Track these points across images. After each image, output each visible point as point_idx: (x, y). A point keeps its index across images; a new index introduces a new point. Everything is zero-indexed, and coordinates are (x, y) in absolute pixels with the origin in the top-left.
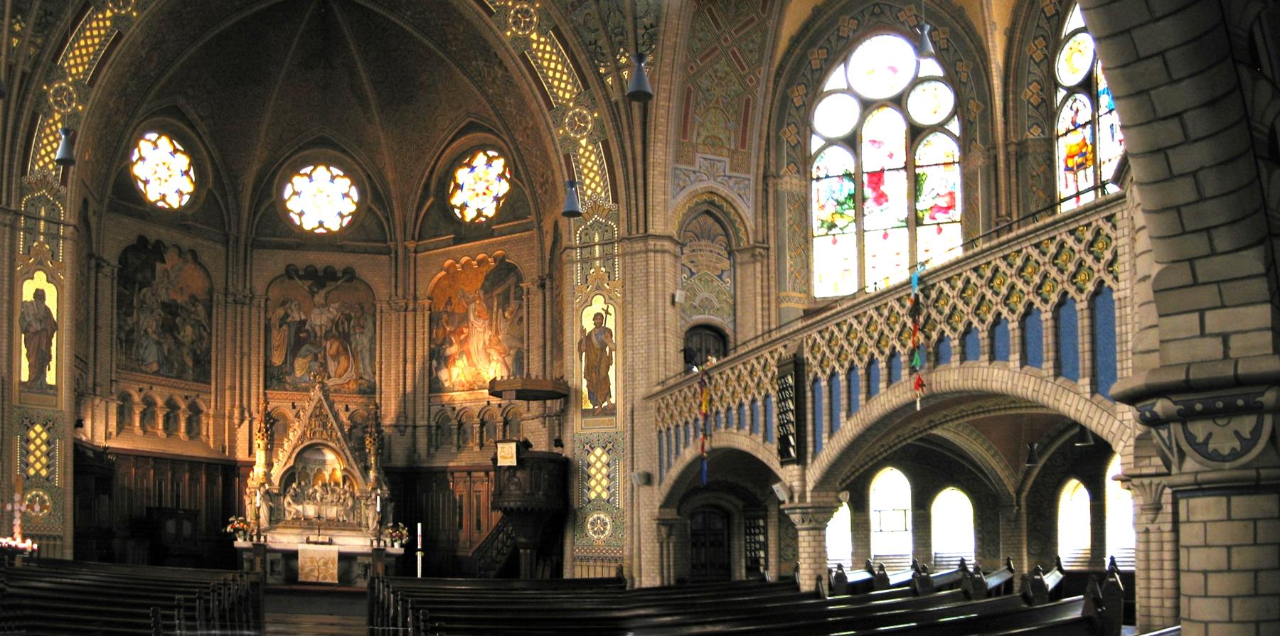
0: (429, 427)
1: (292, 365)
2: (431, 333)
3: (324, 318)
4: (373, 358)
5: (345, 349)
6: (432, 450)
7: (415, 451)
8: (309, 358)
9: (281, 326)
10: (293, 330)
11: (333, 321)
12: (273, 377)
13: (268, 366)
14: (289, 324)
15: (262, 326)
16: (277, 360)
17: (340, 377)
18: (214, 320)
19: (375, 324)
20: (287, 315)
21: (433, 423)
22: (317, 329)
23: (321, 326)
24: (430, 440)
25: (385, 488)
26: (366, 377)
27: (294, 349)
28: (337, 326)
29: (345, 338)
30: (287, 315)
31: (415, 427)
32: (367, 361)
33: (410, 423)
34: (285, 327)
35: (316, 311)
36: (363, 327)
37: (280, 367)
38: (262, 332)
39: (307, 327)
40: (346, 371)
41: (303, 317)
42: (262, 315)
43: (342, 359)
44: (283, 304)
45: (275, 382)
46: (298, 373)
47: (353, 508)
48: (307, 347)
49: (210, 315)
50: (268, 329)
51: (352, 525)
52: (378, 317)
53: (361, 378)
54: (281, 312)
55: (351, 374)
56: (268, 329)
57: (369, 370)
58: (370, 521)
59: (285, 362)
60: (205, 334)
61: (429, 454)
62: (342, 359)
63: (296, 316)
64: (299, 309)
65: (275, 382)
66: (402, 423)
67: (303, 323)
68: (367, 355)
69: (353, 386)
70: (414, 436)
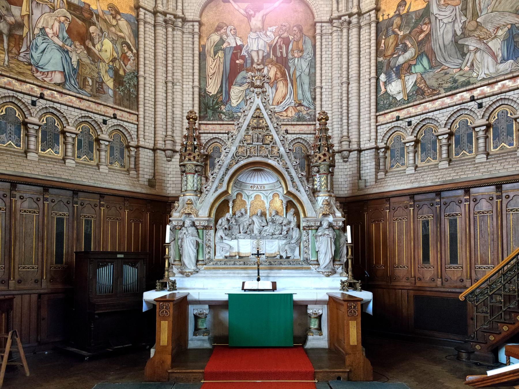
0: (377, 148)
1: (228, 94)
2: (378, 44)
3: (261, 43)
4: (312, 82)
5: (283, 75)
6: (381, 175)
7: (360, 178)
8: (246, 86)
9: (215, 53)
10: (229, 57)
11: (270, 46)
12: (207, 107)
13: (203, 94)
14: (224, 50)
15: (197, 52)
16: (212, 89)
17: (278, 104)
18: (141, 40)
19: (314, 46)
20: (222, 41)
21: (381, 145)
22: (254, 55)
23: (258, 52)
24: (378, 165)
25: (339, 214)
26: (305, 103)
27: (230, 77)
28: (275, 53)
29: (283, 63)
30: (222, 41)
31: (360, 151)
32: (306, 87)
33: (355, 146)
34: (220, 54)
35: (253, 35)
36: (302, 51)
37: (215, 96)
38: (197, 58)
39: (244, 53)
40: (284, 98)
41: (239, 43)
42: (196, 39)
43: (281, 85)
44: (218, 29)
45: (210, 112)
46: (234, 102)
47: (299, 241)
48: (243, 74)
49: (136, 35)
50: (202, 57)
51: (297, 262)
52: (318, 37)
53: (300, 105)
54: (215, 38)
55: (290, 100)
56: (202, 57)
57: (308, 95)
58: (321, 257)
59: (220, 91)
60: (129, 54)
61: (376, 178)
62: (281, 85)
63: (232, 42)
64: (235, 34)
65: (210, 112)
66: (345, 147)
67: (239, 48)
68: (306, 80)
69: (291, 113)
70: (359, 161)
